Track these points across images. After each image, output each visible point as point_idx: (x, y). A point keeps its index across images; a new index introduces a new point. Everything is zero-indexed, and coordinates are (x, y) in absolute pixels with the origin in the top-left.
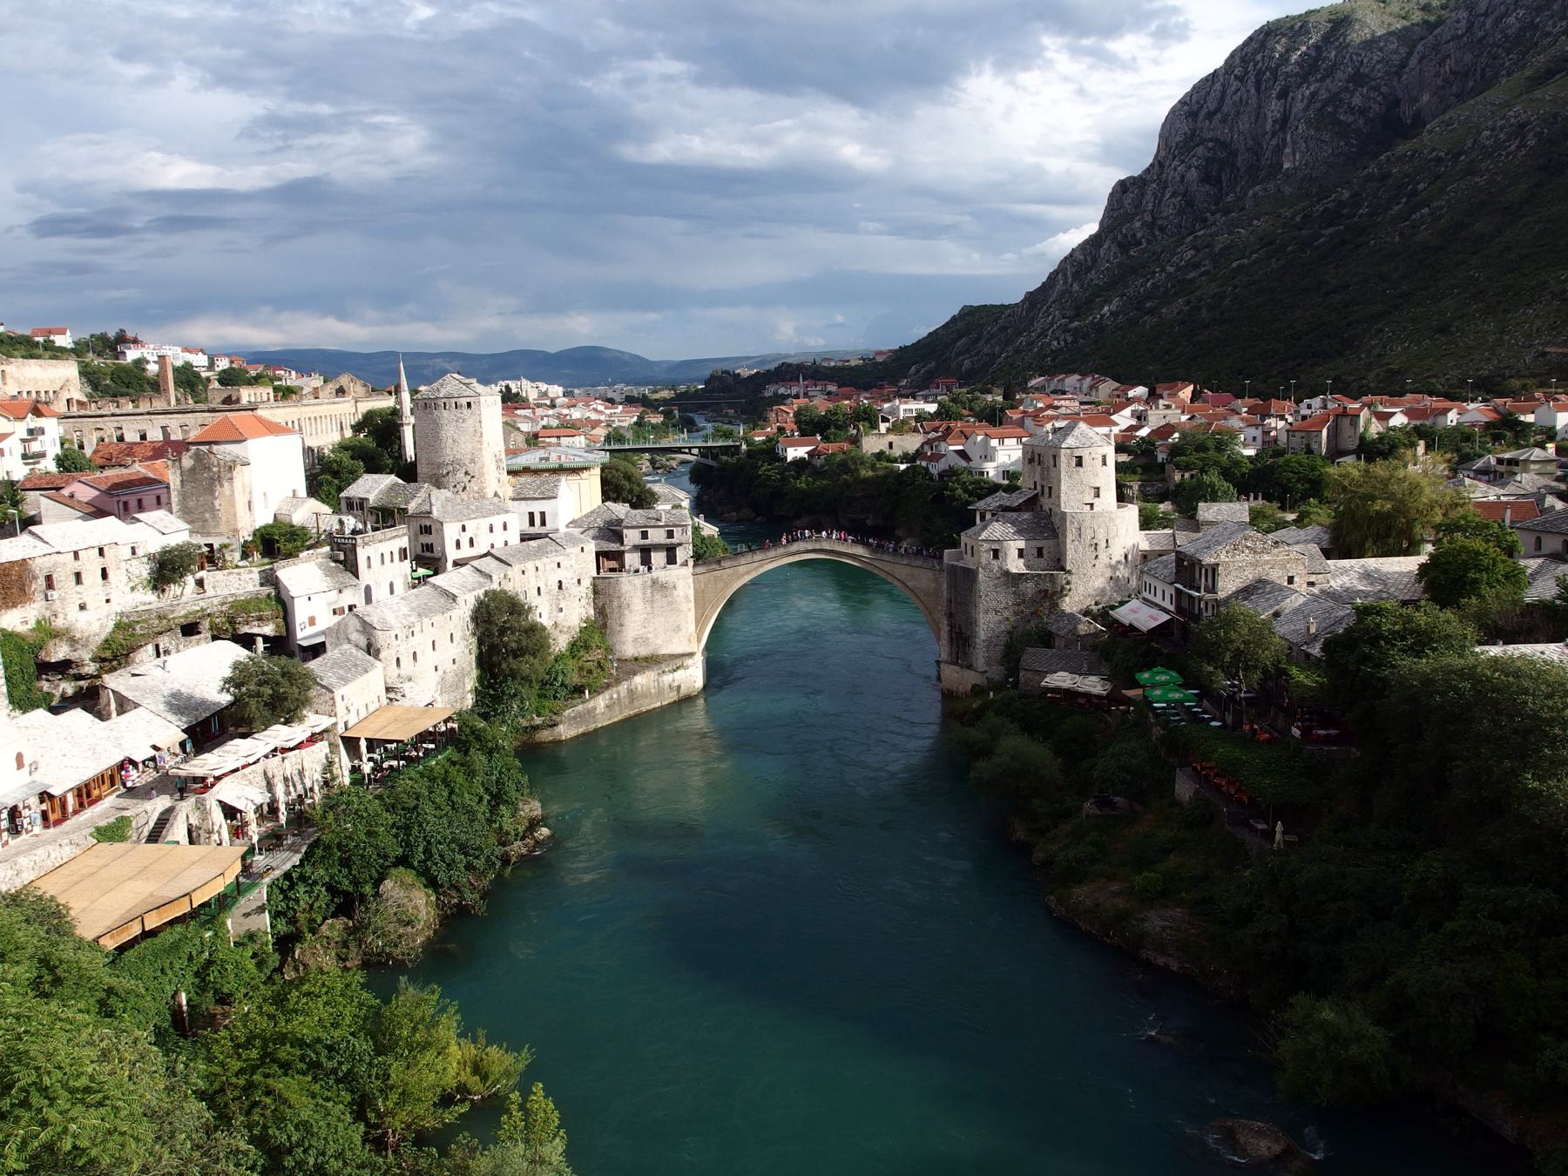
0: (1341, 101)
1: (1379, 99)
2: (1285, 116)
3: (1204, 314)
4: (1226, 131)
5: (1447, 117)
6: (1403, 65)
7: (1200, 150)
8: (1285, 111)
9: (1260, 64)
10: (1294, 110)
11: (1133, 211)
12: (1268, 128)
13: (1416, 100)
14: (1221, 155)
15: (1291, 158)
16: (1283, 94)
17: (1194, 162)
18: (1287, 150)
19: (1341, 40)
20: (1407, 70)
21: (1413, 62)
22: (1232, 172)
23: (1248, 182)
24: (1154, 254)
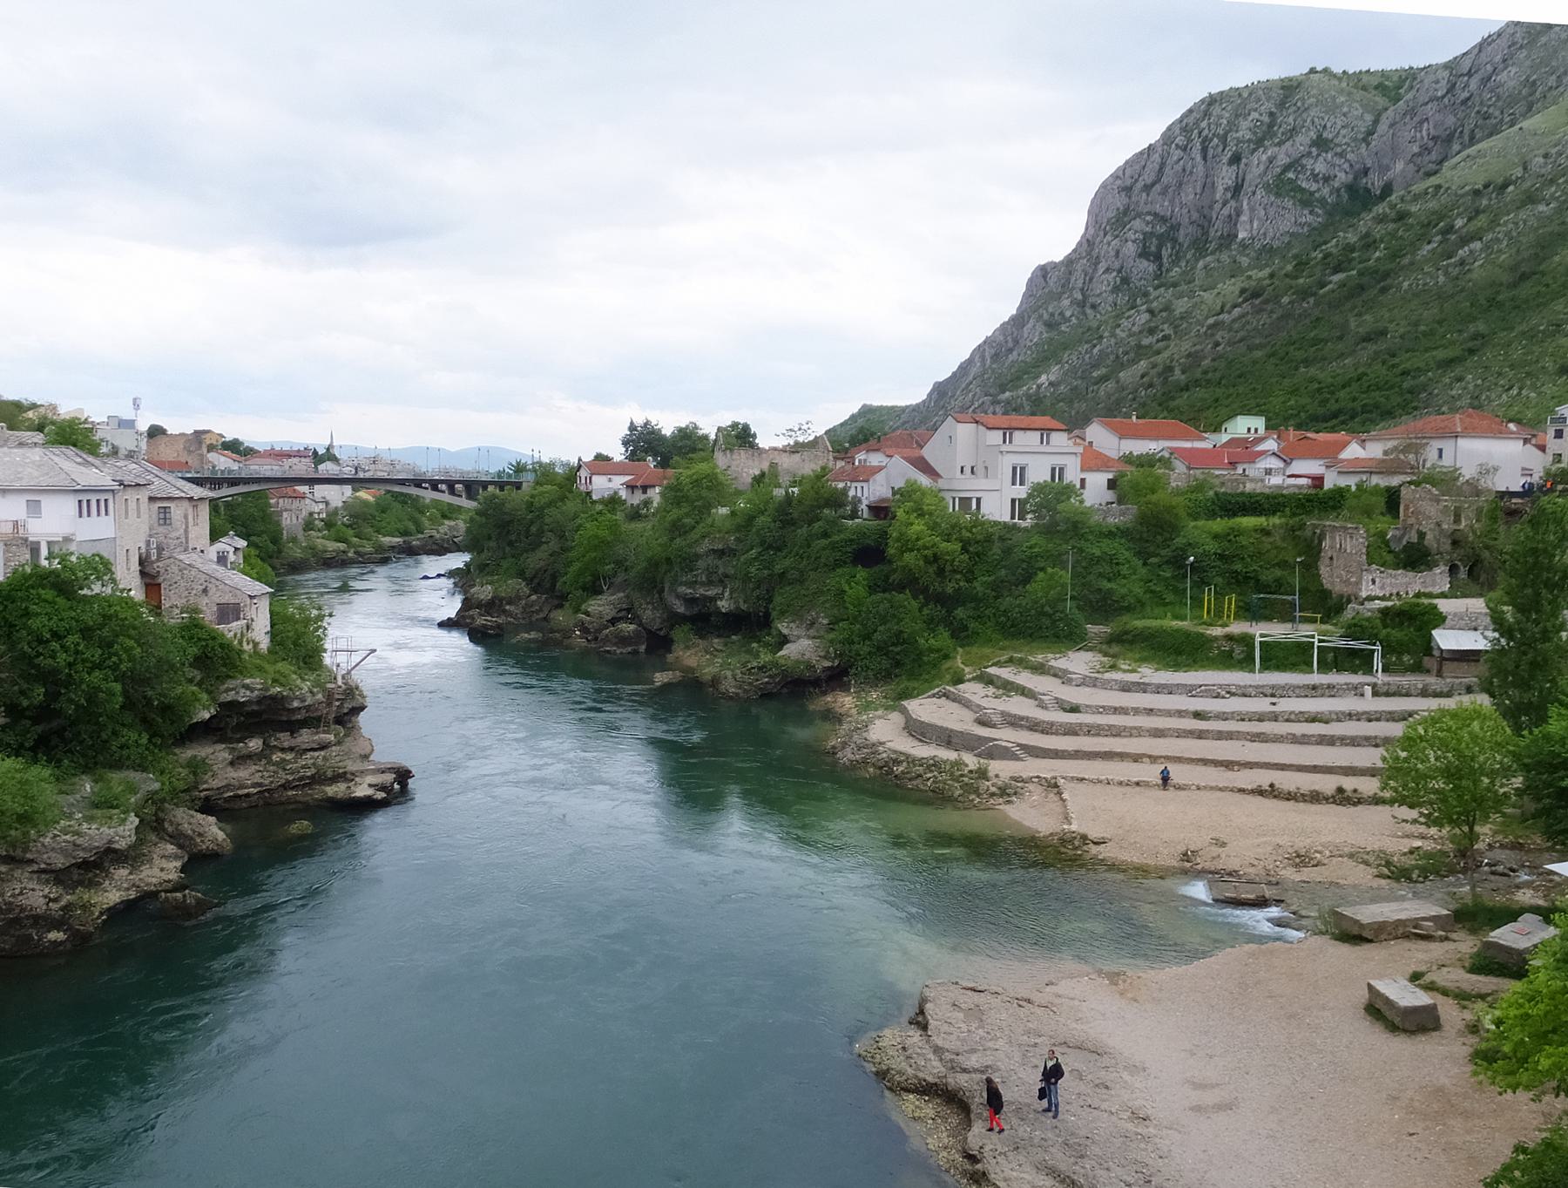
0: (1303, 167)
1: (1346, 166)
2: (1237, 183)
3: (1177, 372)
4: (1166, 204)
5: (1472, 151)
6: (1370, 133)
7: (1137, 224)
8: (1237, 178)
9: (1206, 131)
10: (1248, 178)
11: (1060, 289)
12: (1218, 196)
13: (1388, 168)
14: (1160, 229)
15: (1248, 227)
16: (1236, 159)
17: (1131, 235)
18: (1244, 218)
19: (1299, 104)
20: (1375, 136)
21: (1383, 127)
22: (1172, 249)
23: (1194, 255)
24: (1088, 330)
